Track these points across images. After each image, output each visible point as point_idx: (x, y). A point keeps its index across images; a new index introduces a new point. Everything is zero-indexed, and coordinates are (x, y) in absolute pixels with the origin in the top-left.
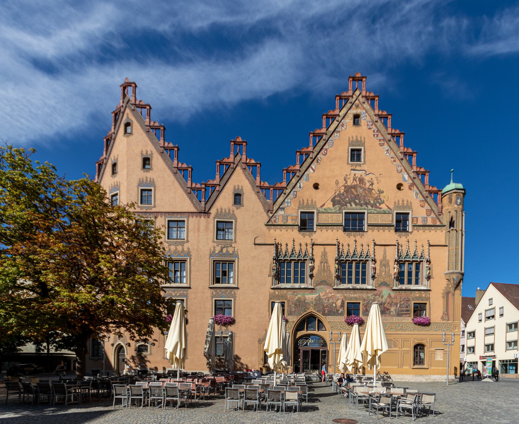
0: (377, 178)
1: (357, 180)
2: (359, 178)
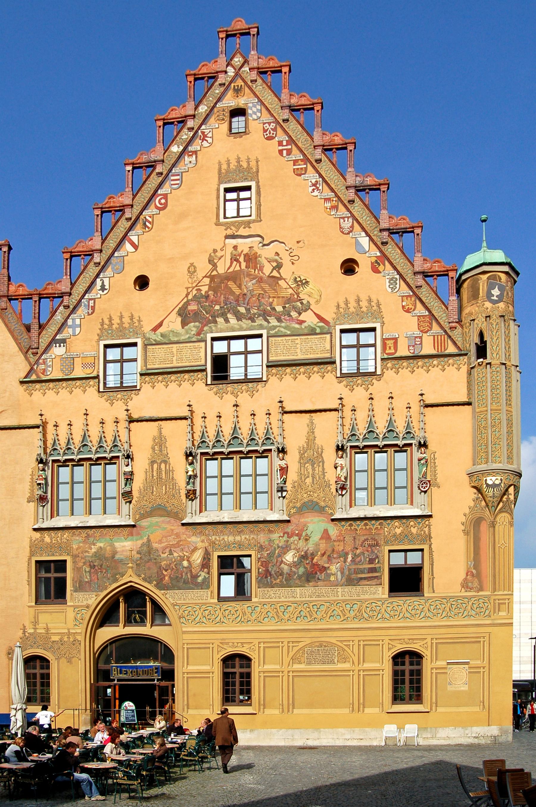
0: (290, 251)
1: (242, 259)
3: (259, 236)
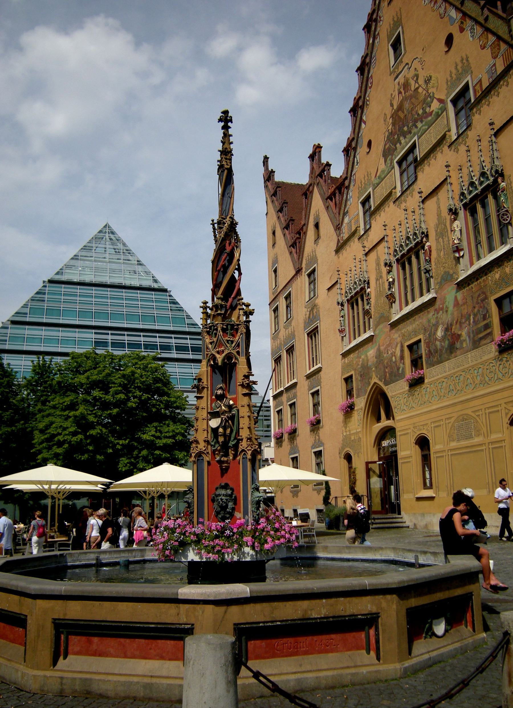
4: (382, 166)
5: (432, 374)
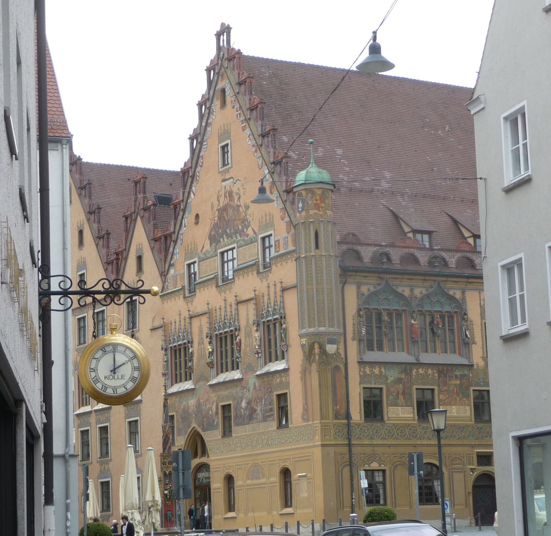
2: (229, 192)
3: (232, 178)
4: (207, 247)
5: (238, 431)
